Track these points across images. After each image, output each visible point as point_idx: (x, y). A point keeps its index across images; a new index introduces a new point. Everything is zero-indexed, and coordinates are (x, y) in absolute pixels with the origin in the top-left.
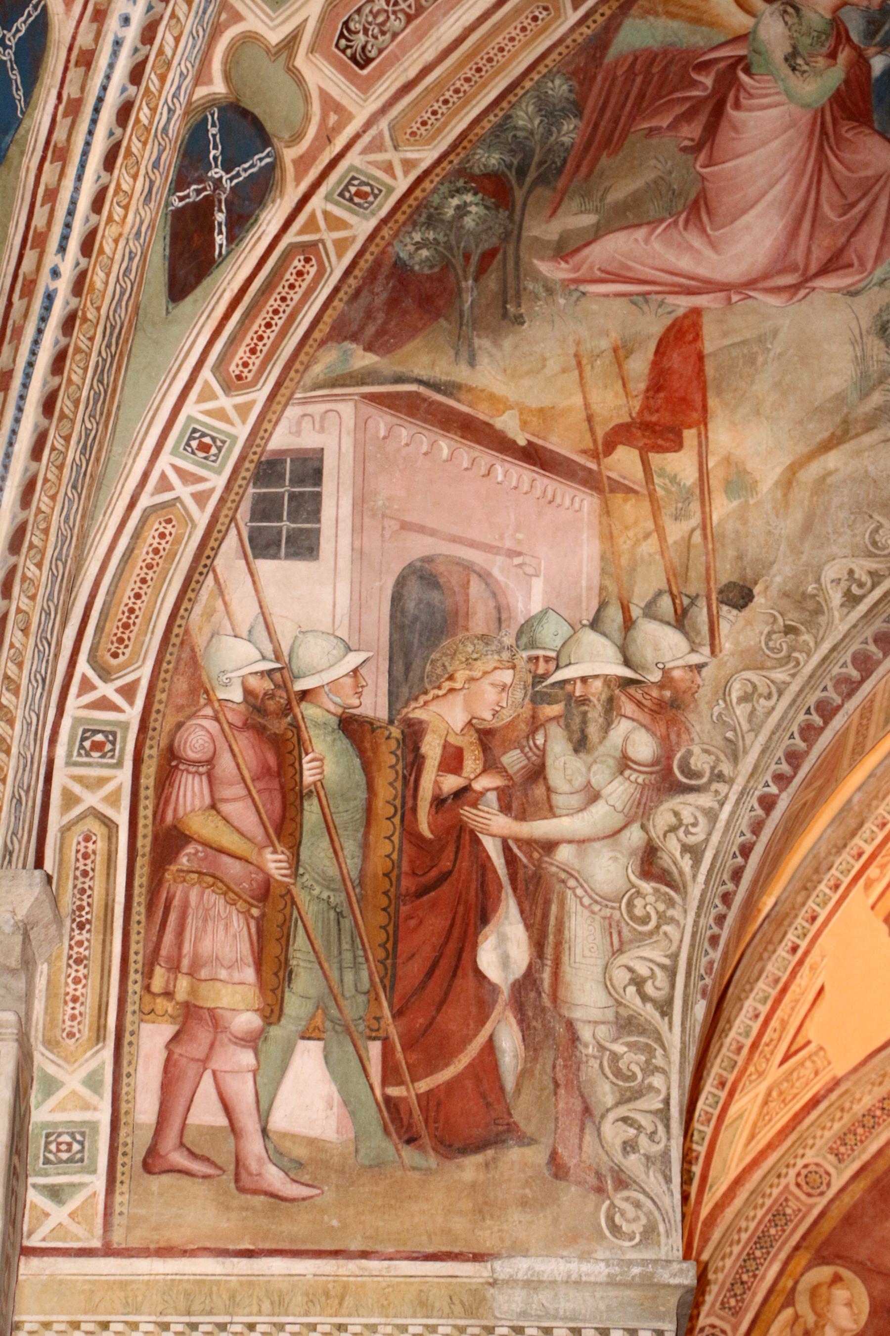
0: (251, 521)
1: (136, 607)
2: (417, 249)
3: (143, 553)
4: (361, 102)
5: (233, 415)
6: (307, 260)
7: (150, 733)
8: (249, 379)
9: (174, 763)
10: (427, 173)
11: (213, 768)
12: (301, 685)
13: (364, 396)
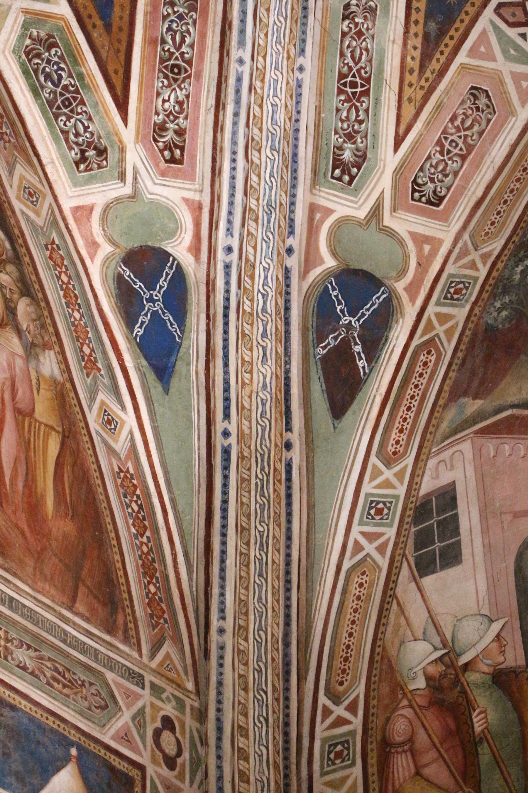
0: (415, 553)
1: (351, 643)
2: (500, 312)
3: (350, 604)
4: (445, 229)
5: (394, 481)
6: (429, 353)
7: (370, 732)
8: (401, 452)
9: (387, 750)
10: (498, 257)
11: (413, 743)
12: (463, 660)
13: (476, 432)
